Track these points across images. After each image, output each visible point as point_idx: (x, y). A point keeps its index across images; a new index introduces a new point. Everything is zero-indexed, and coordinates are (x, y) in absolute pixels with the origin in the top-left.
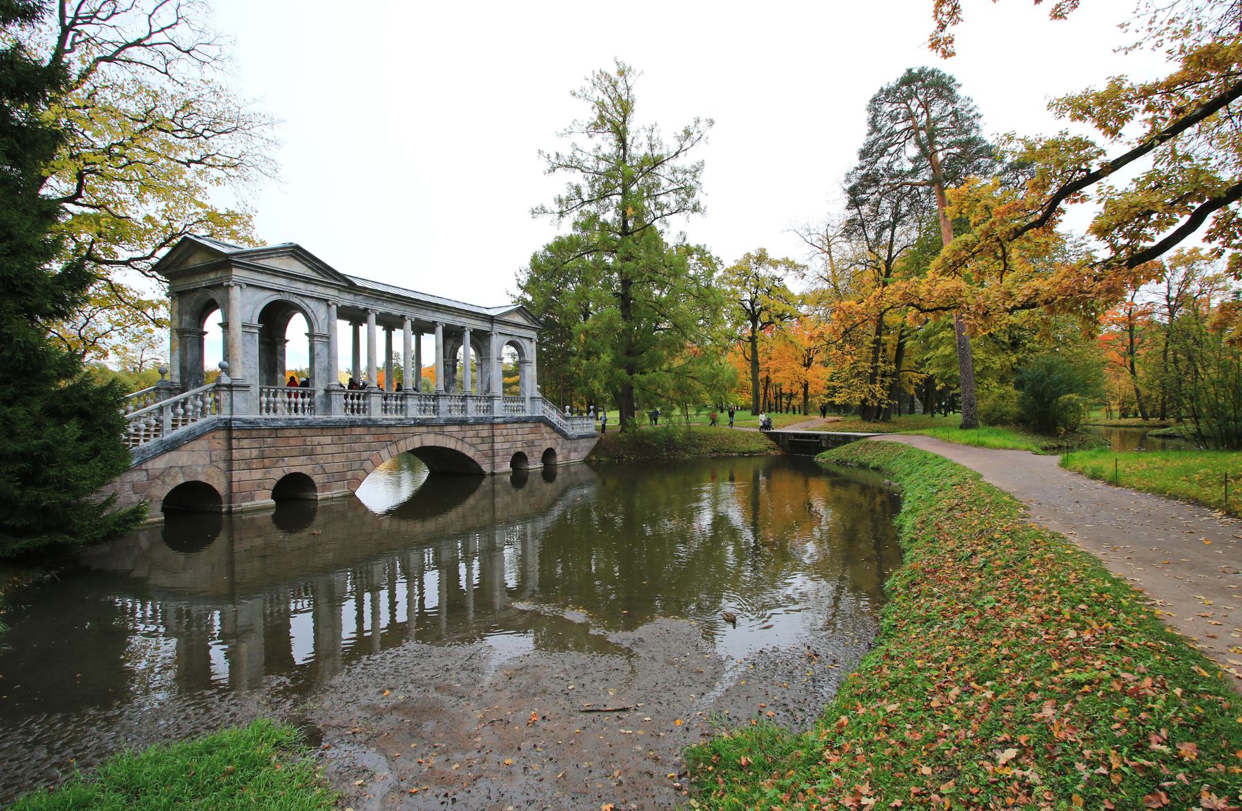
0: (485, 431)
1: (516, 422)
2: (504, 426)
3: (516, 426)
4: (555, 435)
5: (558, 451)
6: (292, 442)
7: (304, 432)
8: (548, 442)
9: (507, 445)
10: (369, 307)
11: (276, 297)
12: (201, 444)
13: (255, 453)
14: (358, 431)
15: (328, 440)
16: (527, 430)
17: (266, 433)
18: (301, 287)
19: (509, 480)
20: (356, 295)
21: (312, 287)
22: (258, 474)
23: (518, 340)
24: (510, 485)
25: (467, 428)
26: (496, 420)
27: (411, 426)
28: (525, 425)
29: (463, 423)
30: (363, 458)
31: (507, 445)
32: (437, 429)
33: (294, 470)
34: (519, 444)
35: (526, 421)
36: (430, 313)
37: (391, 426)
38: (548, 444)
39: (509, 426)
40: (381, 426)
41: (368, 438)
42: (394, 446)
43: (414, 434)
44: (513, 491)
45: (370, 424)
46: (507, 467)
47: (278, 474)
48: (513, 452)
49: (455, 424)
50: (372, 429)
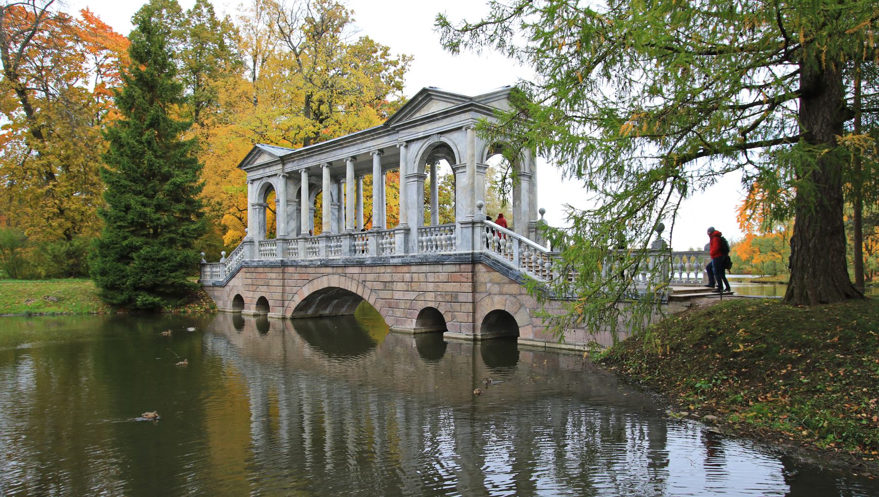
0: (386, 274)
1: (421, 264)
2: (405, 269)
3: (424, 268)
4: (514, 288)
5: (520, 319)
6: (262, 276)
7: (266, 270)
8: (497, 298)
9: (412, 296)
10: (300, 167)
11: (262, 183)
12: (239, 275)
13: (250, 281)
14: (291, 270)
15: (274, 276)
16: (443, 277)
17: (253, 269)
18: (268, 171)
19: (414, 345)
20: (293, 161)
21: (272, 169)
22: (251, 294)
23: (444, 139)
24: (416, 351)
25: (367, 270)
26: (392, 261)
27: (319, 266)
28: (440, 268)
29: (361, 264)
30: (294, 292)
31: (412, 296)
32: (340, 270)
33: (263, 295)
34: (430, 296)
35: (439, 261)
36: (339, 152)
37: (306, 267)
38: (498, 303)
39: (414, 269)
40: (301, 266)
41: (296, 276)
42: (310, 283)
43: (323, 275)
44: (421, 362)
45: (295, 265)
46: (412, 325)
47: (257, 296)
48: (421, 305)
49: (354, 266)
50: (298, 269)
